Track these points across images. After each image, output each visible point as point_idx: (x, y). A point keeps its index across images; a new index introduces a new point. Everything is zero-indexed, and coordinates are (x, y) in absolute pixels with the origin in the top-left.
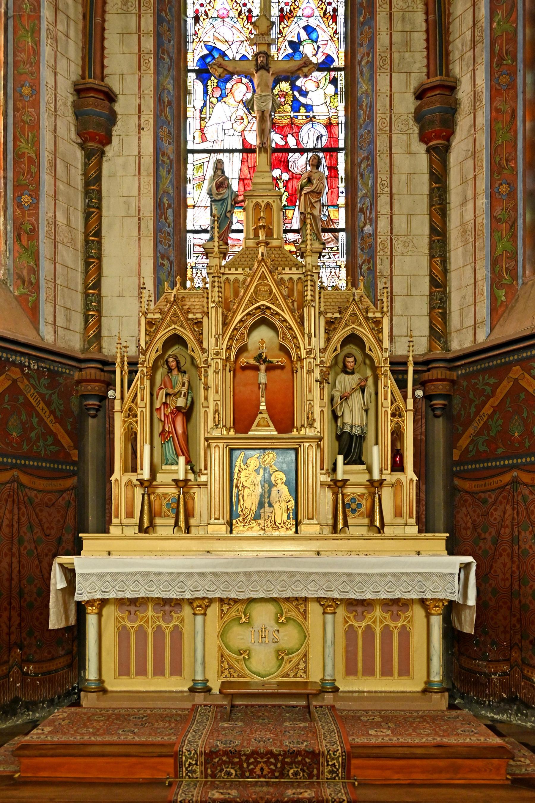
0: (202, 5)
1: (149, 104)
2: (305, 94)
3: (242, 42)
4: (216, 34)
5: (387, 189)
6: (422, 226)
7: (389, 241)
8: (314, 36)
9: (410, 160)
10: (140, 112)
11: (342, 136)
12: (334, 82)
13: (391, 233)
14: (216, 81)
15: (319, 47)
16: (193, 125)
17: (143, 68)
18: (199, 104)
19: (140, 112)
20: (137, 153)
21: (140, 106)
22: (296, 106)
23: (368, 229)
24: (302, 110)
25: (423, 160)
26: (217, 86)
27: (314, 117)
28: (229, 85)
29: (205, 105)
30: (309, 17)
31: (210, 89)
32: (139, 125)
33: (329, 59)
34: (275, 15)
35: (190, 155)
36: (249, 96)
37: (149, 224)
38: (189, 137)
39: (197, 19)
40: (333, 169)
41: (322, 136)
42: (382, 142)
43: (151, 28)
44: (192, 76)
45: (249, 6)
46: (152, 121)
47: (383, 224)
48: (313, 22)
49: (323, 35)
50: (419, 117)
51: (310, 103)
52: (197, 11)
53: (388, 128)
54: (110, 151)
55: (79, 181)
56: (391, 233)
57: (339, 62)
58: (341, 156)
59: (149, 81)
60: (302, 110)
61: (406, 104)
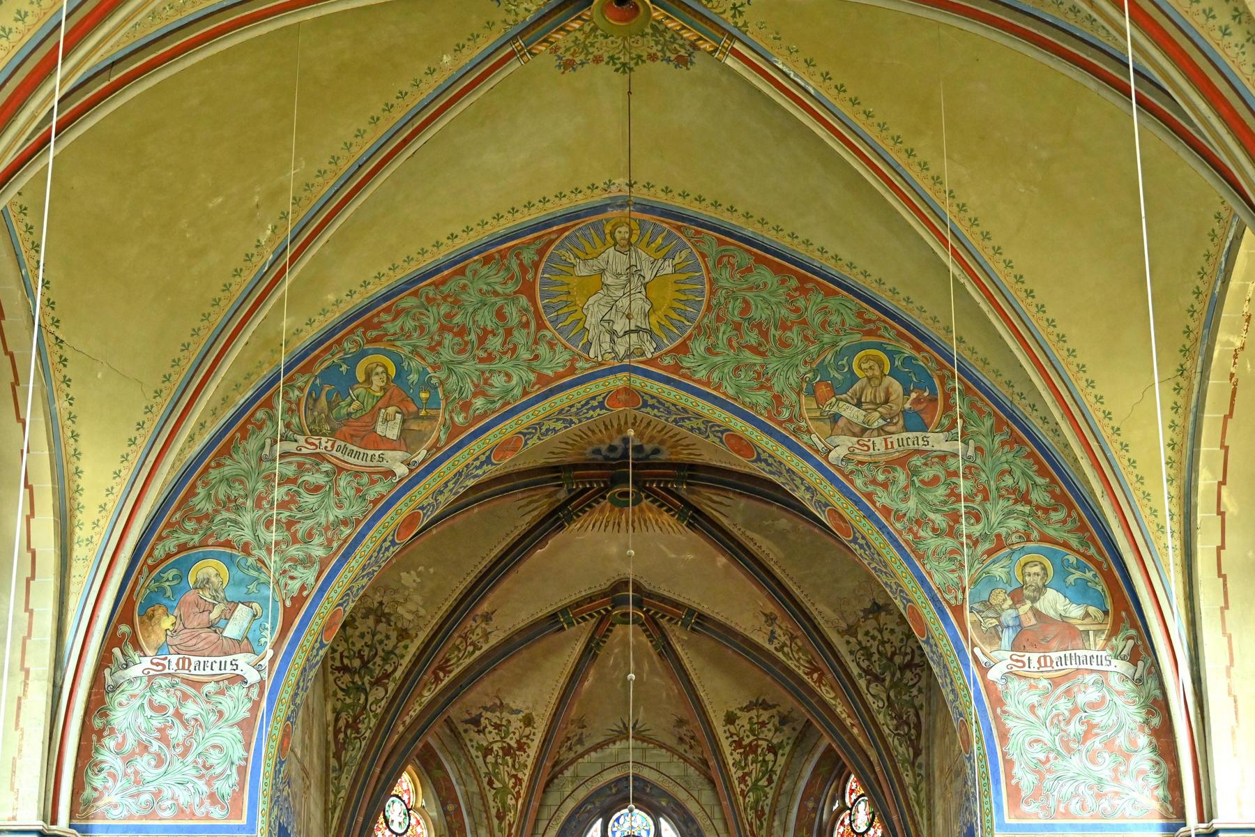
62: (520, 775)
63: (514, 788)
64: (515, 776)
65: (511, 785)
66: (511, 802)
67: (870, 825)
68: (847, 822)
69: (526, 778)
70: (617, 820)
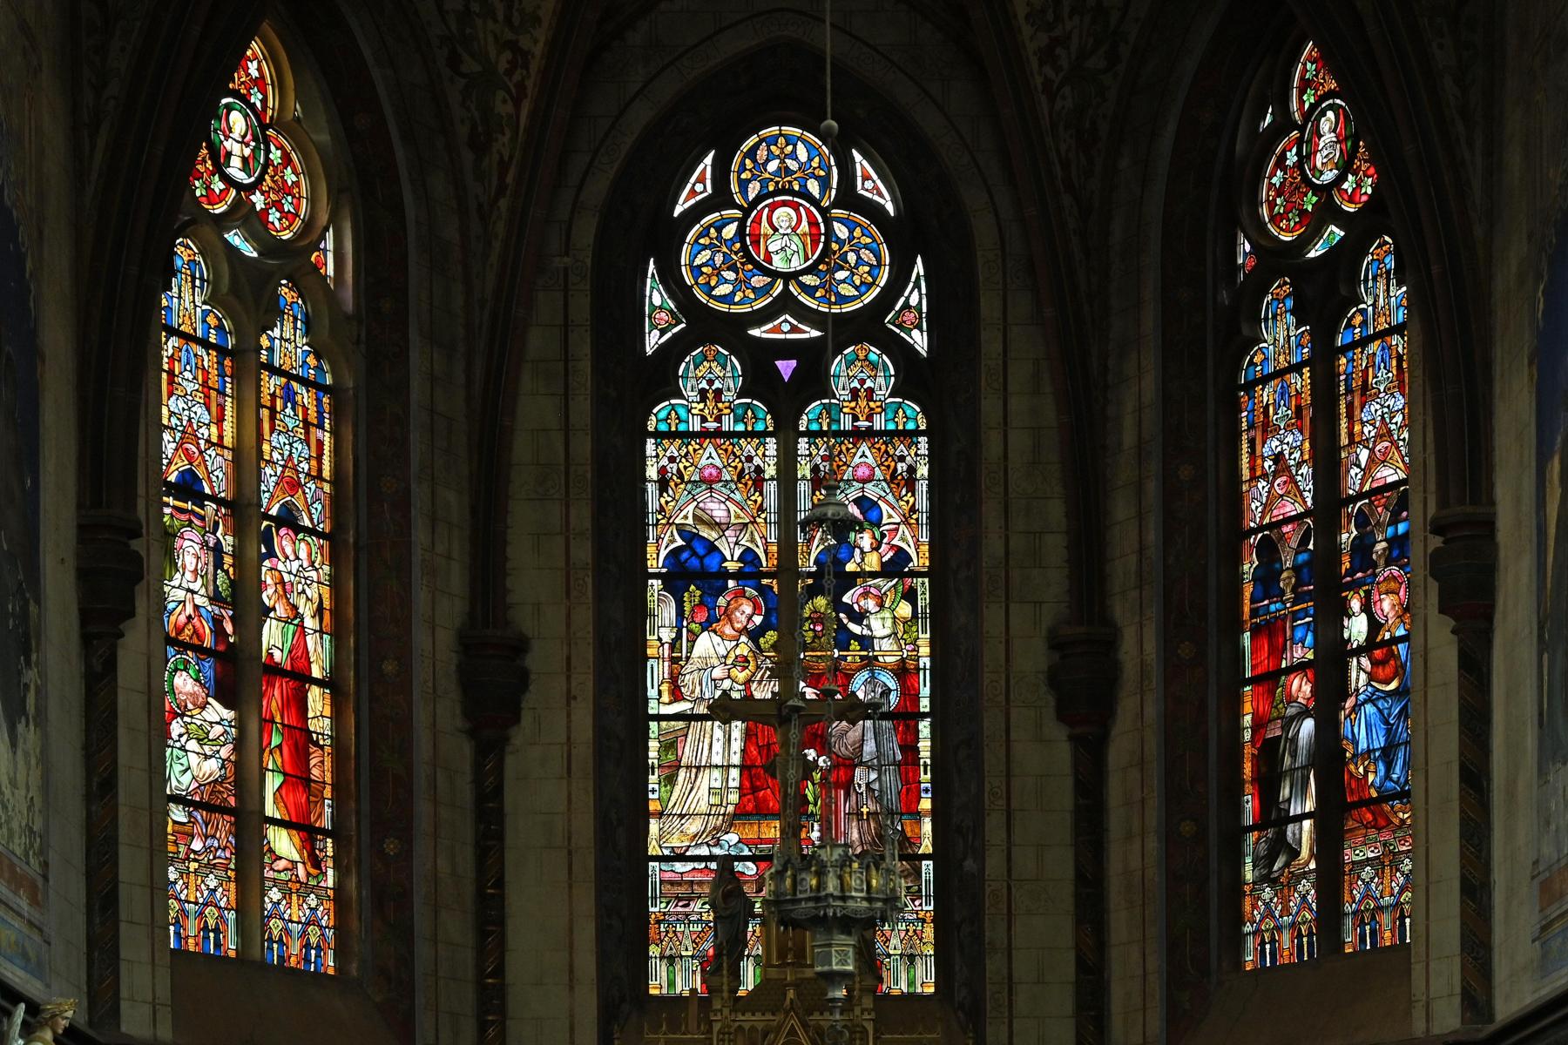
0: (672, 459)
1: (586, 655)
2: (860, 617)
3: (746, 525)
4: (699, 513)
5: (1002, 802)
6: (1062, 865)
7: (1005, 891)
8: (874, 515)
9: (1039, 754)
10: (569, 669)
11: (925, 691)
12: (910, 596)
13: (1009, 875)
14: (698, 593)
15: (883, 536)
16: (657, 671)
17: (574, 593)
18: (667, 635)
19: (569, 669)
20: (563, 739)
21: (569, 659)
22: (844, 638)
23: (969, 864)
24: (855, 645)
25: (1063, 753)
26: (701, 603)
27: (876, 658)
28: (722, 601)
29: (679, 636)
30: (864, 481)
31: (687, 607)
32: (569, 691)
33: (901, 556)
34: (804, 478)
35: (653, 725)
36: (758, 620)
37: (587, 862)
38: (652, 693)
39: (663, 485)
40: (910, 749)
41: (890, 690)
42: (991, 723)
43: (588, 524)
44: (656, 584)
45: (757, 461)
46: (591, 684)
47: (994, 863)
48: (872, 491)
49: (890, 515)
50: (1054, 679)
51: (866, 632)
52: (662, 471)
53: (1002, 698)
54: (520, 736)
55: (466, 793)
56: (1009, 875)
57: (920, 559)
58: (924, 727)
59: (584, 617)
60: (855, 645)
61: (1033, 658)
62: (525, 42)
63: (509, 73)
64: (513, 46)
65: (503, 66)
66: (503, 108)
67: (1345, 168)
68: (1292, 158)
69: (538, 50)
70: (752, 153)
